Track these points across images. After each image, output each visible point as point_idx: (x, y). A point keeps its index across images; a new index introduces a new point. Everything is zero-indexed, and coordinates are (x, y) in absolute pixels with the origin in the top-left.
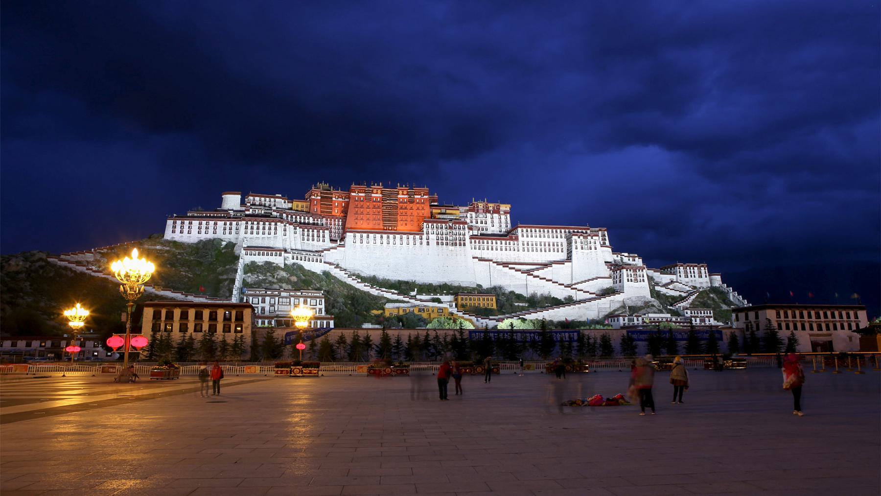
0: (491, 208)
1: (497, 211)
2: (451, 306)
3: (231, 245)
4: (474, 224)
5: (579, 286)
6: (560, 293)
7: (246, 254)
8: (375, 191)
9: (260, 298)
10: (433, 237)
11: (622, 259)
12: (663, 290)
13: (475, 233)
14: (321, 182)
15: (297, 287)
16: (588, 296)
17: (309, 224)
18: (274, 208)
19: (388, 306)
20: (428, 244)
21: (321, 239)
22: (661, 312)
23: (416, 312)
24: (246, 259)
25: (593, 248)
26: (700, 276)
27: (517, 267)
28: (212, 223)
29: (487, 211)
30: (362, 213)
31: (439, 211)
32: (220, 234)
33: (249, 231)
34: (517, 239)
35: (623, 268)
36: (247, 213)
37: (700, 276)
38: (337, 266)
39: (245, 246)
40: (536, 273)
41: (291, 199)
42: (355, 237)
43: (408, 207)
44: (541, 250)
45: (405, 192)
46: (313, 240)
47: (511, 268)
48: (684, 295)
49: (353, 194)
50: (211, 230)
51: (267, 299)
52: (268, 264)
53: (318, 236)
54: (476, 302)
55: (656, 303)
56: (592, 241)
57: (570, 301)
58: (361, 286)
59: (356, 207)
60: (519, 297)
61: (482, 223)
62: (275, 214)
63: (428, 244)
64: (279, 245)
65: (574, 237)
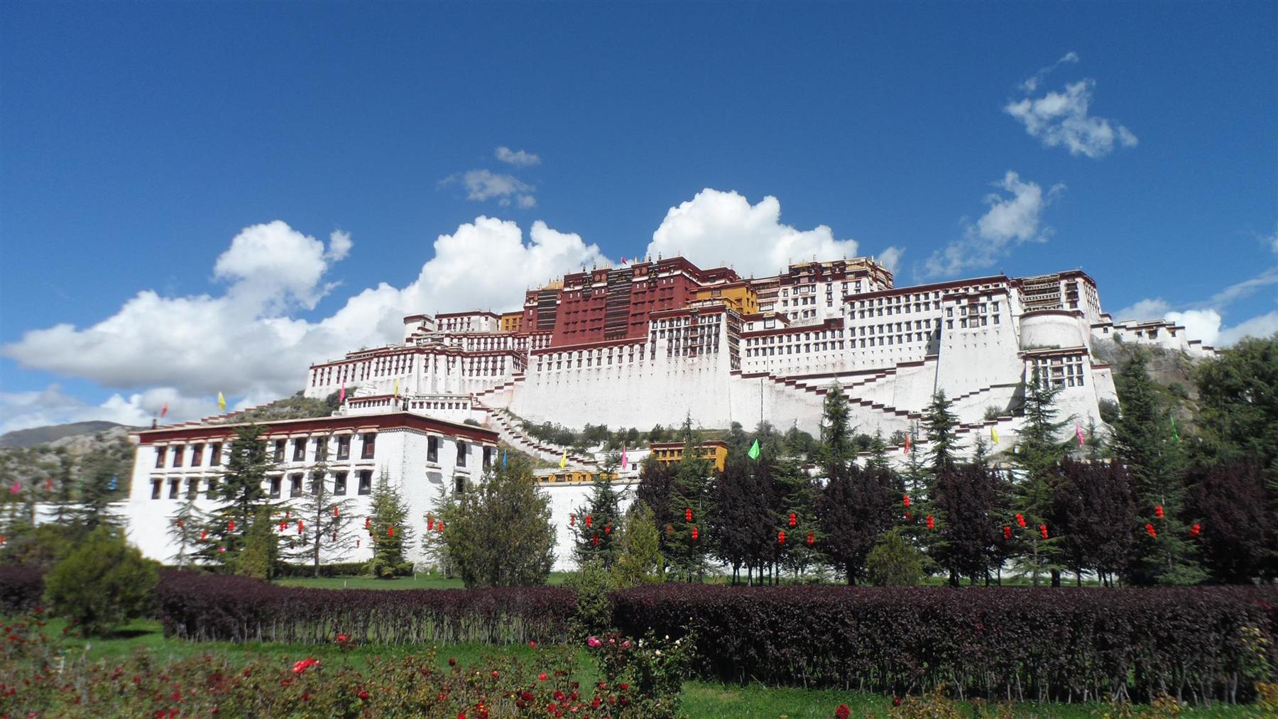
4: (791, 307)
10: (662, 343)
13: (770, 324)
21: (498, 371)
25: (990, 320)
27: (810, 383)
36: (409, 345)
39: (357, 394)
45: (644, 270)
47: (799, 387)
53: (494, 370)
56: (989, 305)
62: (447, 342)
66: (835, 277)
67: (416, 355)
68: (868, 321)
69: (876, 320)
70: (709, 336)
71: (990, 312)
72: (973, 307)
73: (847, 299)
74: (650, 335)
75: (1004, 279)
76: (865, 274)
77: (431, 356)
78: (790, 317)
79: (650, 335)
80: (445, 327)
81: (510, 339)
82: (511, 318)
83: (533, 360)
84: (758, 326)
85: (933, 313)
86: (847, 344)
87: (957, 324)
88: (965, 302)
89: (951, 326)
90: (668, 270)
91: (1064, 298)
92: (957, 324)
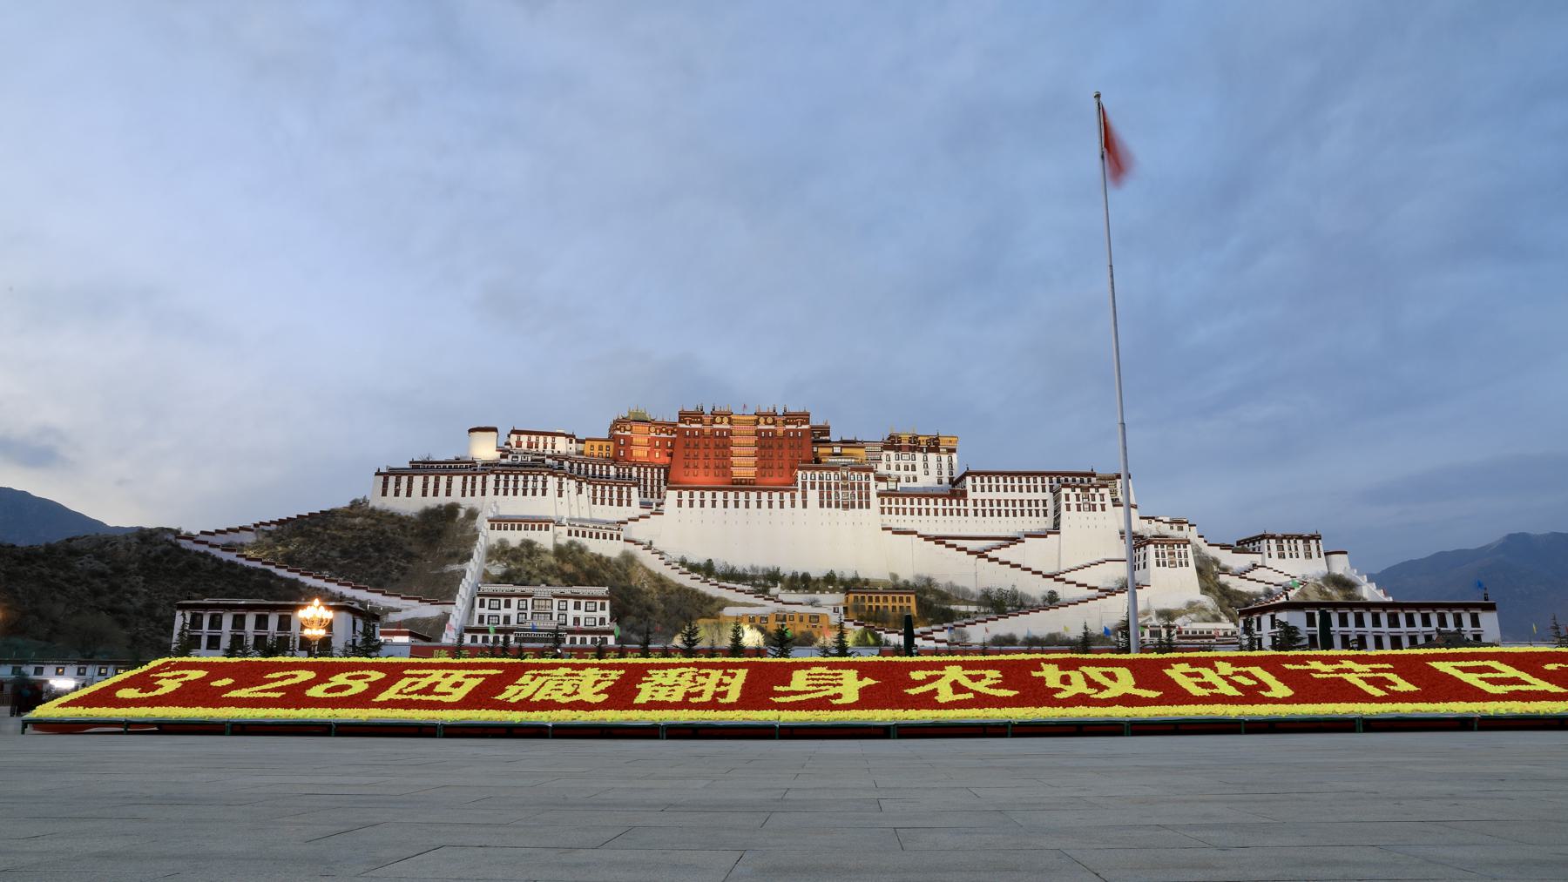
0: (923, 445)
2: (835, 611)
3: (472, 514)
4: (893, 471)
5: (1068, 577)
6: (1036, 588)
7: (492, 528)
8: (718, 419)
9: (503, 600)
10: (813, 496)
12: (1235, 584)
13: (892, 486)
15: (570, 580)
16: (1084, 593)
19: (729, 612)
20: (805, 506)
22: (1217, 619)
25: (1099, 508)
27: (960, 543)
30: (696, 457)
31: (829, 450)
32: (456, 496)
33: (501, 491)
34: (964, 494)
35: (1149, 542)
36: (504, 461)
38: (649, 547)
40: (992, 554)
42: (680, 495)
45: (770, 420)
46: (611, 504)
51: (514, 601)
52: (528, 544)
54: (881, 604)
55: (1208, 602)
56: (1098, 497)
57: (1052, 601)
58: (687, 581)
59: (687, 447)
60: (965, 597)
61: (906, 468)
62: (549, 461)
63: (805, 506)
64: (551, 514)
65: (1065, 491)
66: (929, 450)
68: (987, 495)
69: (994, 495)
70: (860, 497)
71: (1098, 502)
75: (1094, 475)
80: (524, 445)
81: (612, 468)
82: (597, 444)
85: (1040, 496)
86: (971, 513)
87: (1074, 508)
88: (1078, 491)
89: (1068, 509)
92: (1074, 508)
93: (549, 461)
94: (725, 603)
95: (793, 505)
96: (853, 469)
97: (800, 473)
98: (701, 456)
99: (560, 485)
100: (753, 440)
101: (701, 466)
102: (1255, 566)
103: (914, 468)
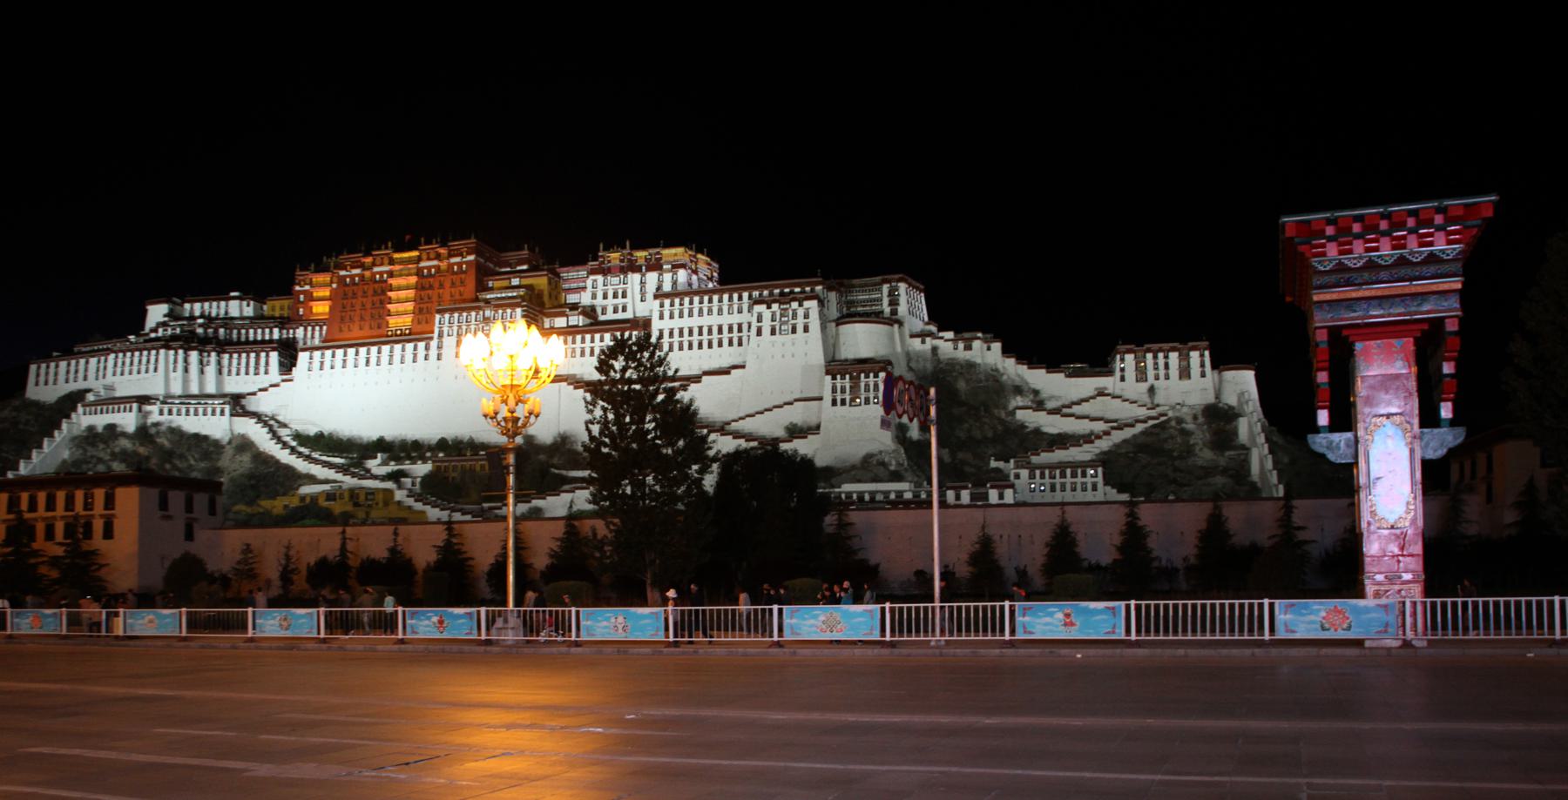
0: (641, 262)
1: (656, 266)
4: (599, 301)
8: (378, 261)
11: (935, 349)
14: (329, 256)
17: (271, 341)
18: (200, 321)
19: (306, 490)
21: (262, 369)
22: (896, 477)
23: (323, 503)
24: (84, 419)
25: (800, 328)
26: (1185, 373)
28: (82, 361)
29: (634, 268)
31: (505, 283)
36: (153, 335)
37: (1185, 373)
41: (260, 298)
43: (436, 285)
44: (700, 346)
48: (1099, 427)
49: (343, 273)
50: (81, 375)
52: (111, 428)
53: (257, 368)
56: (801, 312)
61: (615, 296)
65: (759, 308)
66: (650, 268)
67: (162, 351)
69: (686, 322)
71: (800, 321)
72: (783, 313)
73: (659, 295)
74: (436, 331)
76: (683, 266)
77: (181, 352)
78: (599, 310)
79: (436, 335)
83: (303, 357)
84: (560, 322)
85: (744, 318)
87: (766, 331)
88: (775, 307)
89: (759, 333)
90: (461, 255)
91: (886, 301)
92: (766, 331)
93: (200, 331)
94: (312, 479)
95: (426, 358)
96: (498, 306)
97: (438, 317)
98: (358, 307)
99: (175, 361)
100: (413, 280)
101: (357, 319)
102: (1101, 393)
103: (624, 296)
